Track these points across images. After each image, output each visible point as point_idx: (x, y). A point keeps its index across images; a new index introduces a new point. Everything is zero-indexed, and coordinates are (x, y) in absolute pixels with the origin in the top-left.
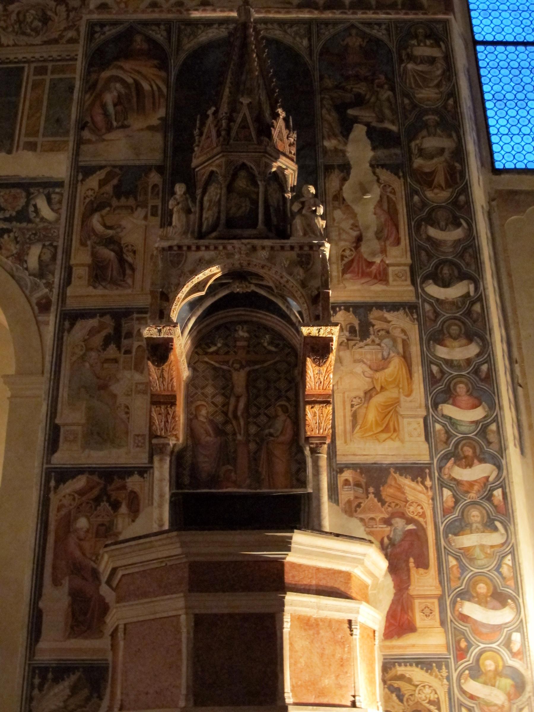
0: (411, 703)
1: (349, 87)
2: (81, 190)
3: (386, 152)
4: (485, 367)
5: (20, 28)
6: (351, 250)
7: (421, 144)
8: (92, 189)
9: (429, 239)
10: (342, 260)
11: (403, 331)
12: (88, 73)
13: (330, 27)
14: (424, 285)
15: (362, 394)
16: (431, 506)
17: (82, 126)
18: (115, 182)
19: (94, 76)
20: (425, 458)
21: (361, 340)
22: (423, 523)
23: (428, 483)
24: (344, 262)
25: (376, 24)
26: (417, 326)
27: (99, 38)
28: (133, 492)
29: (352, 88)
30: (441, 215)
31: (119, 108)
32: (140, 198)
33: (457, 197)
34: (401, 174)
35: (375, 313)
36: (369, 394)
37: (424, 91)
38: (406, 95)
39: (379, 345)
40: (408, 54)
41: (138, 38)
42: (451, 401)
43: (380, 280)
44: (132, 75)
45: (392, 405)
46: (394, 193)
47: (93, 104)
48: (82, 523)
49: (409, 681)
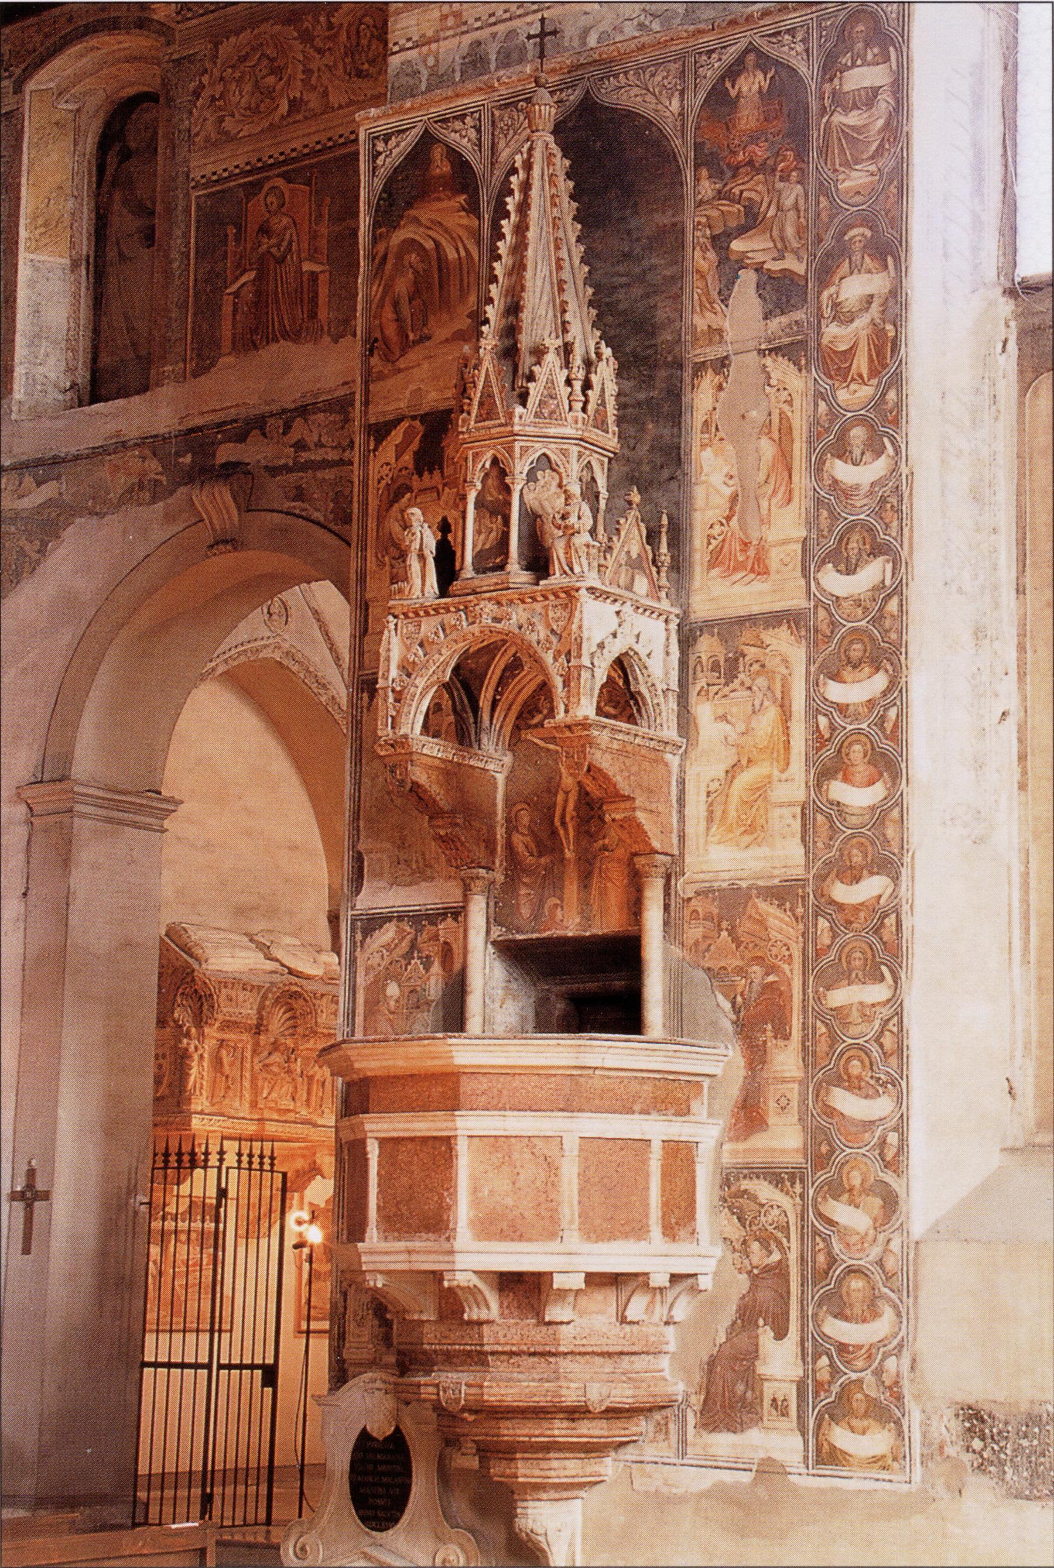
0: (754, 1228)
1: (736, 191)
2: (375, 469)
3: (784, 320)
4: (892, 713)
5: (353, 61)
6: (722, 524)
7: (838, 293)
8: (388, 464)
9: (835, 482)
10: (709, 543)
11: (785, 661)
12: (375, 240)
13: (714, 56)
14: (819, 575)
15: (722, 775)
16: (801, 945)
17: (371, 346)
18: (415, 446)
19: (381, 248)
20: (799, 872)
21: (726, 684)
22: (788, 972)
23: (800, 910)
24: (711, 547)
25: (788, 31)
26: (804, 650)
27: (387, 163)
28: (445, 943)
29: (742, 192)
30: (858, 434)
31: (417, 302)
32: (448, 471)
33: (884, 395)
34: (803, 362)
35: (747, 636)
36: (732, 772)
37: (854, 174)
38: (823, 190)
39: (750, 688)
40: (834, 93)
41: (438, 152)
42: (840, 775)
43: (759, 574)
44: (431, 233)
45: (758, 789)
46: (790, 403)
47: (381, 306)
48: (393, 990)
49: (754, 1198)
